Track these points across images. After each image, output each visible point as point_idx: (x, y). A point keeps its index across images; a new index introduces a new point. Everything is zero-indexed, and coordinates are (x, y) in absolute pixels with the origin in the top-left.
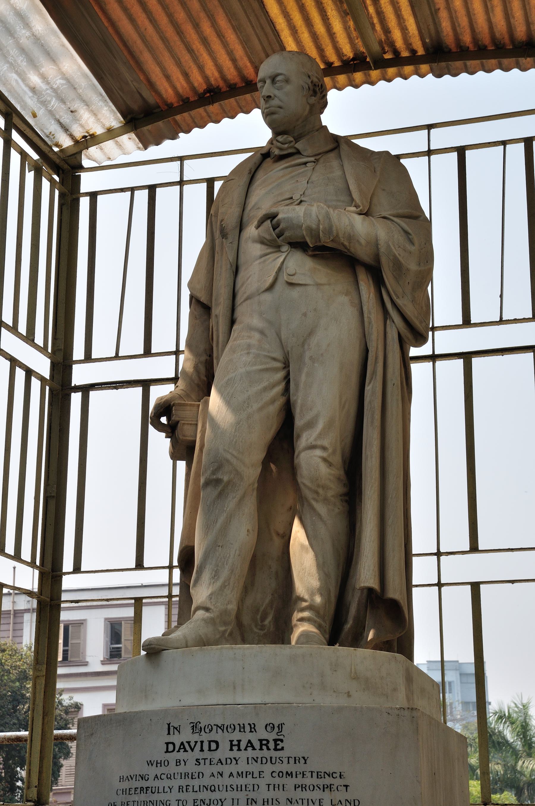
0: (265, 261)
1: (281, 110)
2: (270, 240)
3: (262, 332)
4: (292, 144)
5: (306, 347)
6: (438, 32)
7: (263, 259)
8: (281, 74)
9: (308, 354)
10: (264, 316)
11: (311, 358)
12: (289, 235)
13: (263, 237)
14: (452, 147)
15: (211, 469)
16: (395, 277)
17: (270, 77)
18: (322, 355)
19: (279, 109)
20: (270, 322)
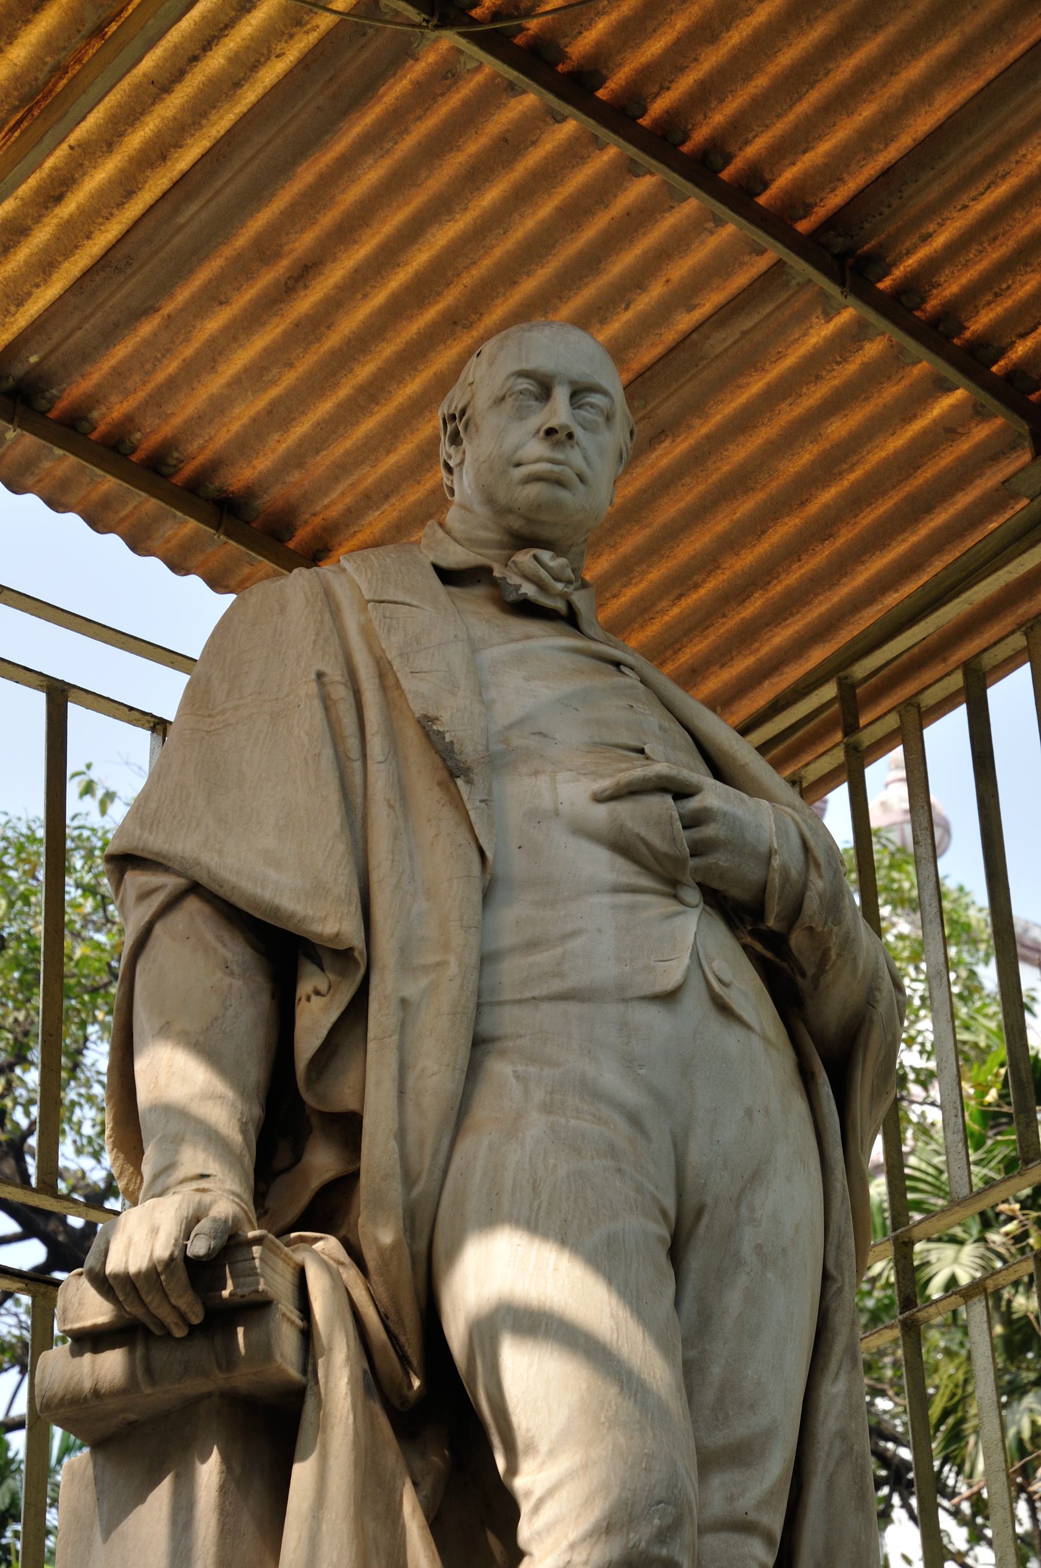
0: (632, 908)
1: (581, 487)
2: (667, 855)
3: (634, 1120)
4: (570, 589)
5: (744, 1211)
6: (87, 356)
7: (625, 898)
9: (748, 1239)
10: (640, 1072)
11: (759, 1248)
12: (725, 864)
13: (638, 835)
14: (41, 674)
15: (656, 1522)
16: (872, 1095)
17: (572, 383)
18: (784, 1250)
19: (576, 479)
20: (660, 1098)
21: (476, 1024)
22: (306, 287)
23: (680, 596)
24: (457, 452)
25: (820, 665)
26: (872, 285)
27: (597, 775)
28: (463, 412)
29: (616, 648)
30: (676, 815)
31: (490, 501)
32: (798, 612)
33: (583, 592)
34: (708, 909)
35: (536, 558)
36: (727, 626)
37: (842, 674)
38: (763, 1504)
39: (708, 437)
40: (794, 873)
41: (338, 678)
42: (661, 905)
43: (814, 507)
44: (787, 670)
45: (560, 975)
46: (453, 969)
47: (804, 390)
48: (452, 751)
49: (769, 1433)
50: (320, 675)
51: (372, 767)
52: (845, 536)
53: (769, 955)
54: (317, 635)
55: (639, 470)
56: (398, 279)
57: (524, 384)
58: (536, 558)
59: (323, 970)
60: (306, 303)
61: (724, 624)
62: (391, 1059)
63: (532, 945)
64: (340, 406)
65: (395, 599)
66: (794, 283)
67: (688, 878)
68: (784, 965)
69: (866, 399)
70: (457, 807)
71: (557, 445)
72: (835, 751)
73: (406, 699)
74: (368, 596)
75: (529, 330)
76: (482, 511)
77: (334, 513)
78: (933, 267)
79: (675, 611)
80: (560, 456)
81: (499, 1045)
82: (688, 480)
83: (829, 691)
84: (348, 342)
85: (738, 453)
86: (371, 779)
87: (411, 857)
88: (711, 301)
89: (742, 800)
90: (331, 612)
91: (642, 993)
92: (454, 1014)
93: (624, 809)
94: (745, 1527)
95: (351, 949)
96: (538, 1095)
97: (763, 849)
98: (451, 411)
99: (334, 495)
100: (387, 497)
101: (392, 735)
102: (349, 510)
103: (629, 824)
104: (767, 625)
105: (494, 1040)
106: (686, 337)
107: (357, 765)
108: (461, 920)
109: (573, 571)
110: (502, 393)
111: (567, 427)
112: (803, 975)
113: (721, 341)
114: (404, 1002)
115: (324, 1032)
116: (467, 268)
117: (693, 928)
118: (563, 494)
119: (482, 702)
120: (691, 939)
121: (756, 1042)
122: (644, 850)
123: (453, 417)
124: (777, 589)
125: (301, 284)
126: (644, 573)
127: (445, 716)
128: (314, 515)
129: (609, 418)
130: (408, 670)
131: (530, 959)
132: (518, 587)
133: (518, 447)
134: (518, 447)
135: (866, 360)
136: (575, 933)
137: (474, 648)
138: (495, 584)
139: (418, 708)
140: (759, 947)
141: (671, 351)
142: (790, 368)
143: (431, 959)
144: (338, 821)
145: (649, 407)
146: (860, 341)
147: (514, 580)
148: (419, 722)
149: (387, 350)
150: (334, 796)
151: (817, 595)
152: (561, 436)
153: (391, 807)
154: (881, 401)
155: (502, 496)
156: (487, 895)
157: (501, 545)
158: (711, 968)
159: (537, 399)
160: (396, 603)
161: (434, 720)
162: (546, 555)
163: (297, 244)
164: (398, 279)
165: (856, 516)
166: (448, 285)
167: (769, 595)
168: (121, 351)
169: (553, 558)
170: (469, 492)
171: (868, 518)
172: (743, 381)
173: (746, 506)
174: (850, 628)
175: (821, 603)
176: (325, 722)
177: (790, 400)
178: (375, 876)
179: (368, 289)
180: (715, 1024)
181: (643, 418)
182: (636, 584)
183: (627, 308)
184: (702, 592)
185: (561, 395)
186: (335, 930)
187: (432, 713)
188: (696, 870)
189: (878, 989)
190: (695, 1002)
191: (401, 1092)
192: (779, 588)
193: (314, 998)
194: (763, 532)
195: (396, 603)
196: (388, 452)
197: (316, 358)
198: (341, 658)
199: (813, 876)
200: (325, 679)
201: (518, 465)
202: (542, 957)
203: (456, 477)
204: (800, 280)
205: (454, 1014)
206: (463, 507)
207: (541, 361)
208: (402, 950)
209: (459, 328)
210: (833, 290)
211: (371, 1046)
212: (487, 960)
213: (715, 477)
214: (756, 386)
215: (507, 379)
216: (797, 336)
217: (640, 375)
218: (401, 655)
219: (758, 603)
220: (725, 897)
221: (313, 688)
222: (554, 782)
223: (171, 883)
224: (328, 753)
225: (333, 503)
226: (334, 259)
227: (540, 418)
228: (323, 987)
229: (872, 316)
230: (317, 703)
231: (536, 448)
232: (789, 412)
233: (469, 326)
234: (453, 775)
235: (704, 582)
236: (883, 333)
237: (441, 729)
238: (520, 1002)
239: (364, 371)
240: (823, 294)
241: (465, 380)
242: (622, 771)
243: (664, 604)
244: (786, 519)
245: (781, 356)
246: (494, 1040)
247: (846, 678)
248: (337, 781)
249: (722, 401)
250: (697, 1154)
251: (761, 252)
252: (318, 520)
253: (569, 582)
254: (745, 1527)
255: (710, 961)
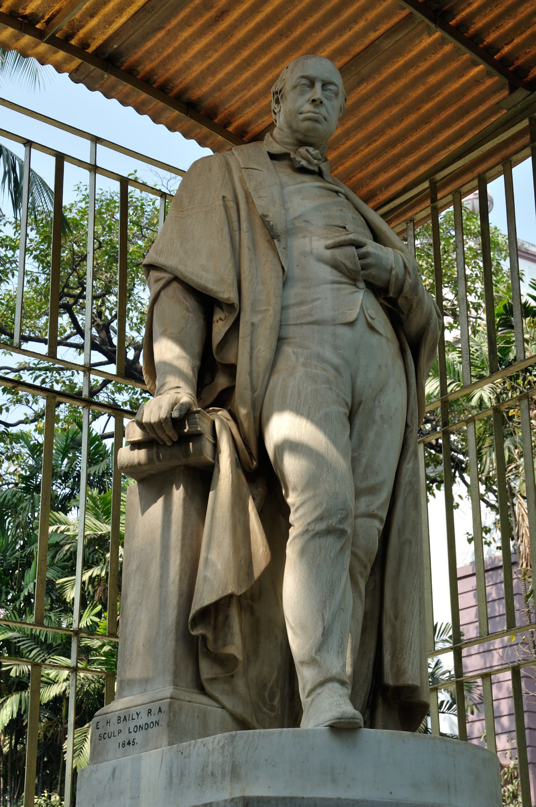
1: (325, 122)
2: (352, 270)
3: (337, 369)
5: (377, 403)
6: (136, 45)
7: (336, 286)
8: (335, 85)
9: (378, 413)
11: (381, 416)
13: (342, 262)
14: (118, 174)
15: (339, 516)
18: (391, 417)
19: (323, 119)
20: (346, 361)
21: (279, 332)
22: (223, 20)
23: (369, 145)
24: (278, 107)
25: (423, 174)
26: (448, 23)
27: (327, 238)
28: (281, 91)
29: (337, 185)
30: (356, 255)
31: (290, 127)
32: (415, 152)
33: (325, 163)
34: (367, 290)
35: (307, 150)
36: (387, 157)
37: (431, 178)
38: (379, 508)
39: (381, 82)
40: (400, 277)
41: (231, 199)
42: (349, 289)
43: (422, 111)
44: (410, 174)
45: (311, 315)
46: (271, 312)
47: (420, 64)
48: (273, 229)
49: (383, 483)
50: (224, 197)
51: (243, 234)
52: (435, 122)
53: (390, 306)
54: (223, 181)
55: (354, 94)
56: (259, 18)
57: (304, 81)
58: (307, 150)
59: (223, 311)
60: (223, 26)
61: (386, 156)
62: (248, 345)
63: (301, 303)
64: (236, 67)
65: (253, 167)
66: (416, 21)
67: (360, 278)
68: (396, 310)
69: (444, 68)
70: (274, 250)
71: (316, 106)
72: (427, 209)
73: (256, 208)
74: (242, 166)
75: (307, 59)
76: (286, 130)
77: (233, 109)
78: (472, 16)
79: (367, 150)
80: (317, 111)
81: (287, 341)
82: (373, 99)
83: (426, 184)
84: (239, 42)
85: (393, 89)
86: (242, 238)
87: (256, 269)
88: (384, 28)
89: (382, 249)
90: (228, 171)
91: (341, 322)
92: (271, 329)
93: (337, 252)
94: (372, 516)
95: (233, 304)
96: (302, 360)
97: (389, 267)
98: (276, 90)
99: (233, 102)
100: (254, 103)
101: (250, 221)
102: (239, 108)
103: (339, 258)
104: (403, 157)
105: (286, 338)
106: (373, 42)
107: (237, 233)
108: (274, 294)
109: (321, 155)
110: (295, 85)
111: (320, 99)
112: (403, 313)
113: (387, 44)
114: (253, 324)
115: (223, 334)
116: (287, 14)
117: (361, 298)
118: (318, 126)
119: (285, 209)
120: (360, 301)
121: (384, 340)
122: (344, 267)
123: (277, 93)
124: (407, 142)
125: (221, 19)
126: (355, 135)
127: (271, 215)
128: (225, 109)
129: (337, 95)
130: (257, 196)
131: (300, 309)
132: (300, 162)
133: (302, 106)
134: (302, 106)
135: (444, 52)
136: (317, 299)
137: (282, 186)
138: (291, 160)
139: (260, 211)
140: (386, 304)
141: (367, 47)
142: (414, 55)
143: (263, 308)
144: (229, 255)
145: (358, 70)
146: (442, 45)
147: (299, 159)
148: (260, 217)
149: (255, 45)
150: (228, 245)
151: (423, 145)
152: (318, 102)
153: (249, 249)
154: (450, 69)
155: (294, 125)
156: (285, 284)
157: (293, 145)
158: (368, 313)
159: (309, 87)
160: (253, 169)
161: (266, 216)
162: (311, 149)
163: (219, 3)
164: (259, 18)
165: (439, 114)
166: (279, 20)
167: (404, 145)
168: (150, 44)
169: (313, 151)
170: (282, 123)
171: (444, 115)
172: (395, 60)
173: (396, 110)
174: (436, 158)
175: (424, 148)
176: (225, 217)
177: (414, 68)
178: (243, 276)
179: (247, 21)
180: (368, 333)
181: (355, 74)
182: (352, 140)
183: (350, 30)
184: (378, 143)
185: (318, 86)
186: (228, 296)
187: (265, 213)
188: (363, 275)
189: (431, 319)
190: (361, 326)
191: (251, 358)
192: (408, 142)
193: (219, 321)
194: (402, 120)
195: (253, 169)
196: (255, 85)
197: (226, 47)
198: (232, 191)
199: (408, 277)
200: (226, 199)
201: (301, 113)
202: (305, 308)
203: (277, 116)
204: (419, 20)
205: (271, 329)
206: (280, 129)
207: (311, 72)
208: (252, 304)
209: (283, 37)
210: (432, 25)
211: (241, 340)
212: (284, 308)
213: (384, 98)
214: (401, 62)
215: (298, 79)
216: (417, 43)
217: (355, 57)
218: (254, 190)
219: (400, 148)
220: (374, 285)
221: (221, 202)
222: (311, 240)
223: (167, 276)
224: (226, 228)
225: (232, 105)
226: (234, 9)
227: (309, 95)
228: (223, 317)
229: (447, 36)
230: (222, 208)
231: (308, 107)
232: (414, 73)
233: (287, 37)
234: (273, 238)
235: (378, 139)
236: (452, 42)
237: (269, 220)
238: (296, 324)
239: (245, 54)
240: (428, 26)
241: (282, 77)
242: (337, 237)
243: (362, 147)
244: (411, 115)
245: (410, 51)
246: (286, 338)
247: (433, 179)
248: (229, 239)
249: (387, 68)
250: (360, 381)
251: (404, 9)
252: (226, 111)
253: (319, 160)
254: (372, 516)
255: (367, 309)
